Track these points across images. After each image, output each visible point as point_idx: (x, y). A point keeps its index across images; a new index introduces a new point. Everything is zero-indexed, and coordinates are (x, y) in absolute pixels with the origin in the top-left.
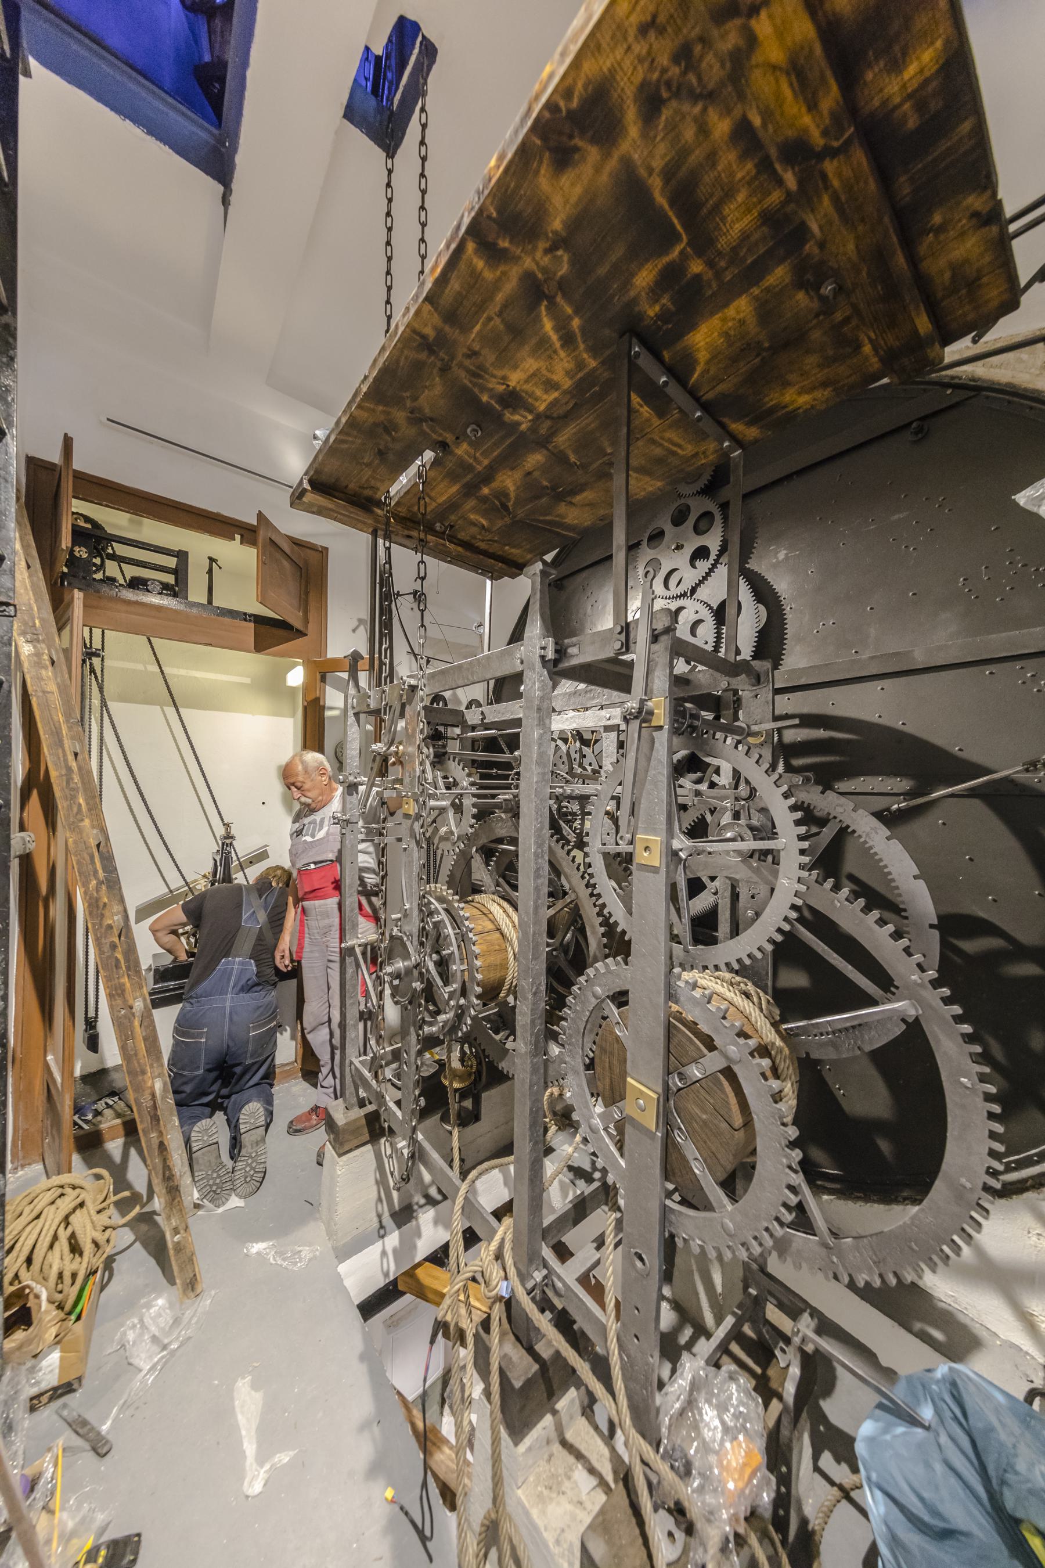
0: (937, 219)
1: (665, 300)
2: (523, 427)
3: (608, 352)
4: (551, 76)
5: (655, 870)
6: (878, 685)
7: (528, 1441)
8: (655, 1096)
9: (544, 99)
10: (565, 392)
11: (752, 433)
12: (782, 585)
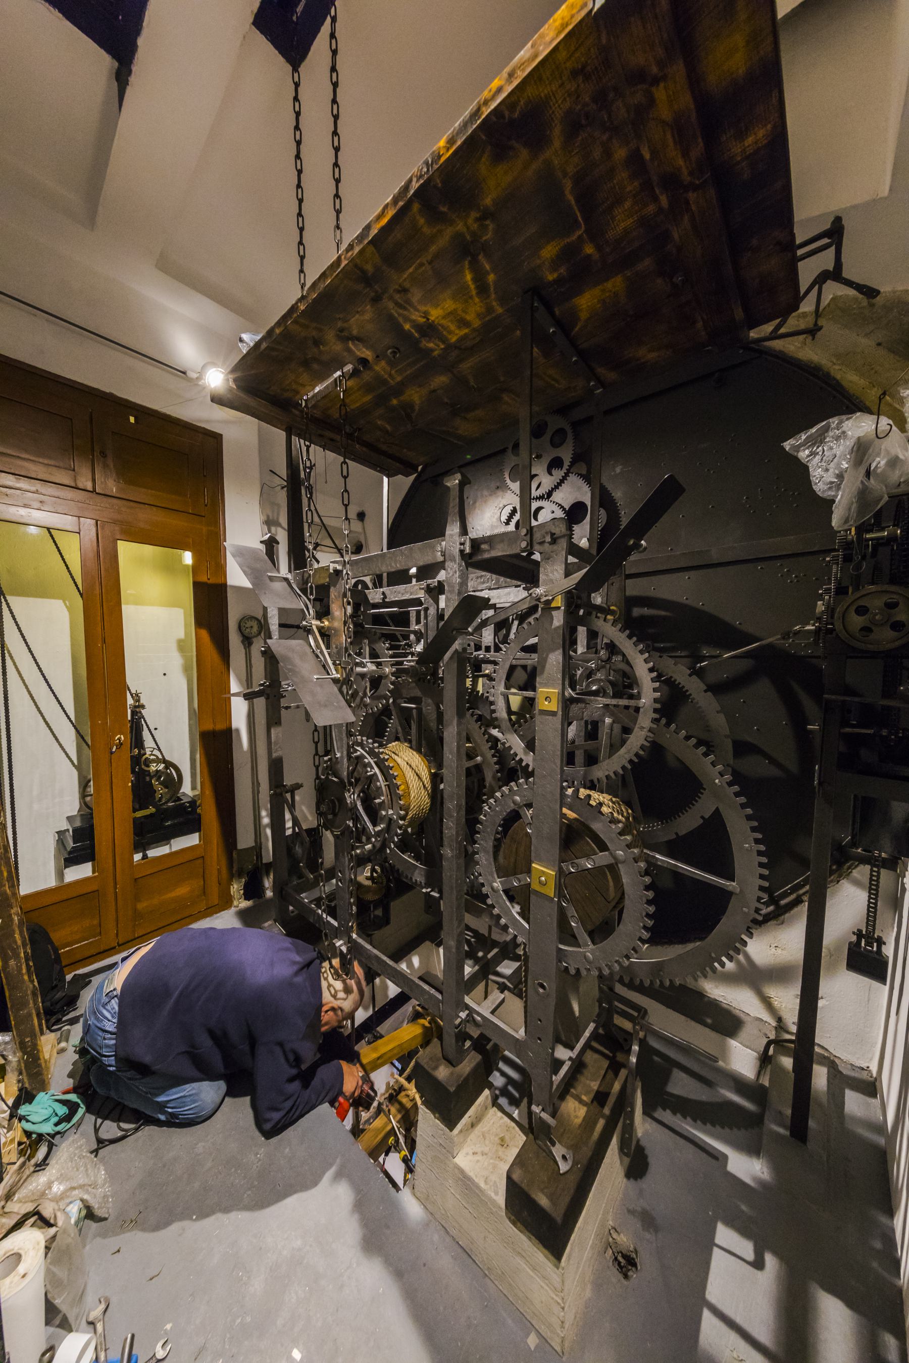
0: (755, 242)
1: (562, 270)
2: (436, 353)
4: (500, 90)
5: (553, 714)
6: (686, 575)
7: (459, 1127)
8: (554, 873)
9: (493, 105)
10: (474, 330)
11: (611, 376)
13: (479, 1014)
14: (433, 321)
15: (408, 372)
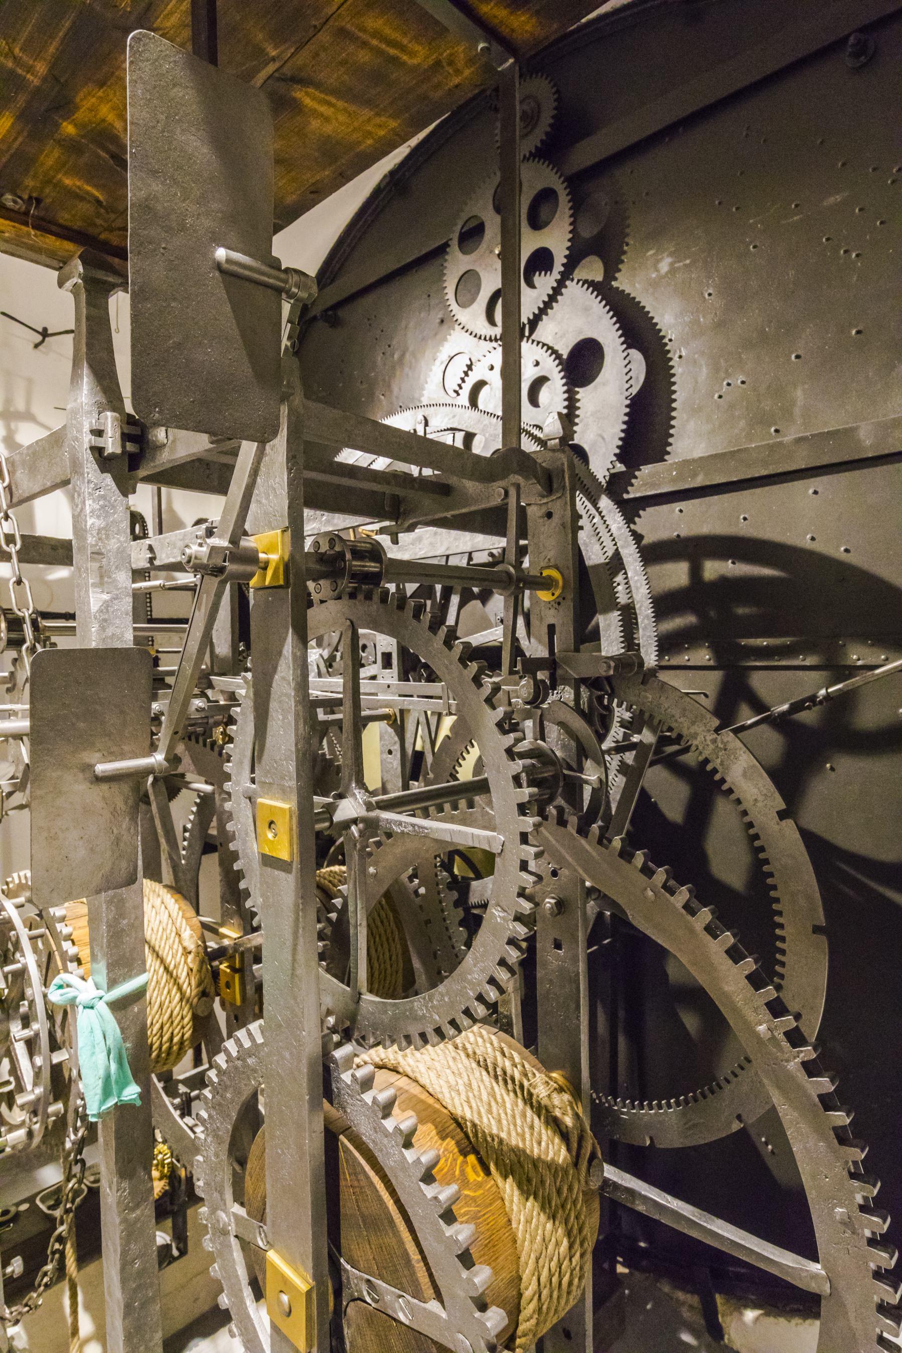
12: (668, 317)
15: (52, 49)
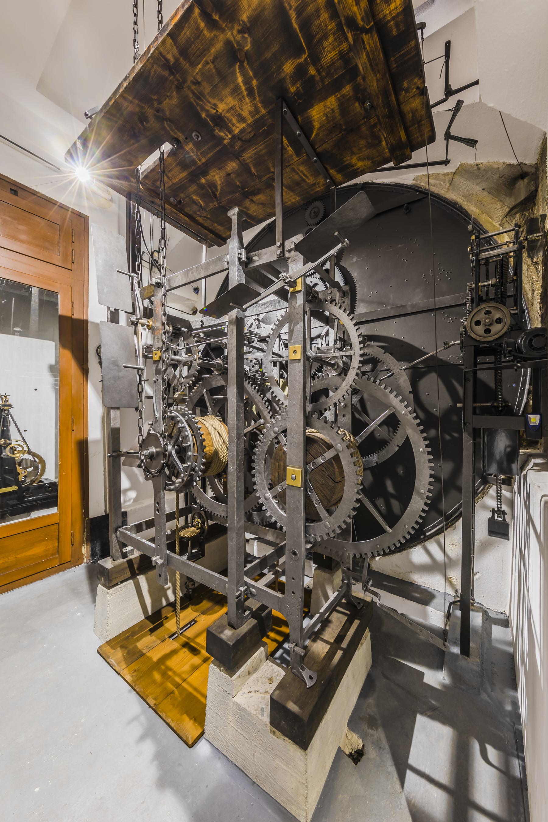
3: (271, 107)
13: (254, 587)
14: (221, 114)
